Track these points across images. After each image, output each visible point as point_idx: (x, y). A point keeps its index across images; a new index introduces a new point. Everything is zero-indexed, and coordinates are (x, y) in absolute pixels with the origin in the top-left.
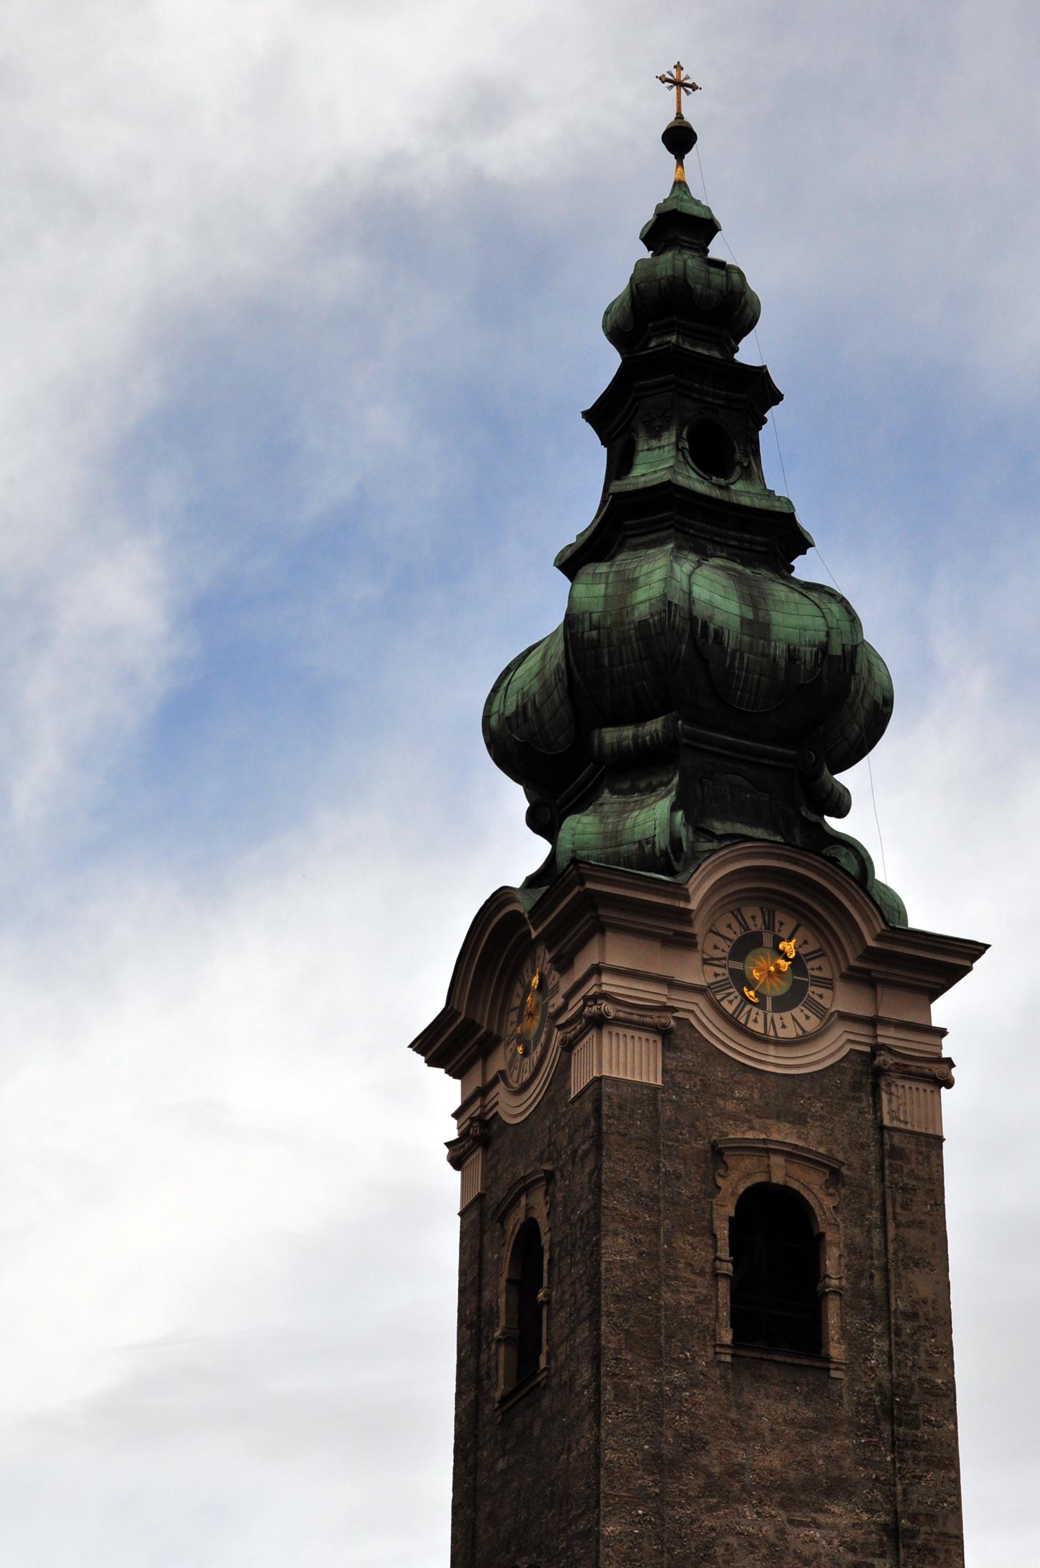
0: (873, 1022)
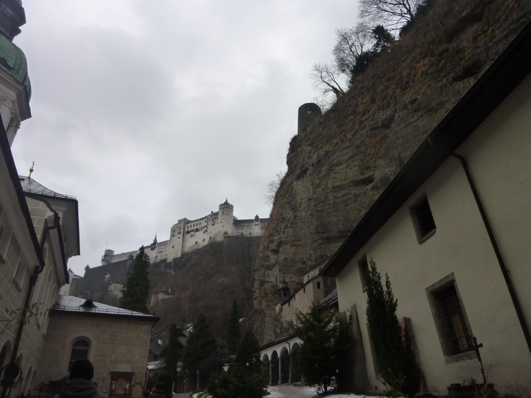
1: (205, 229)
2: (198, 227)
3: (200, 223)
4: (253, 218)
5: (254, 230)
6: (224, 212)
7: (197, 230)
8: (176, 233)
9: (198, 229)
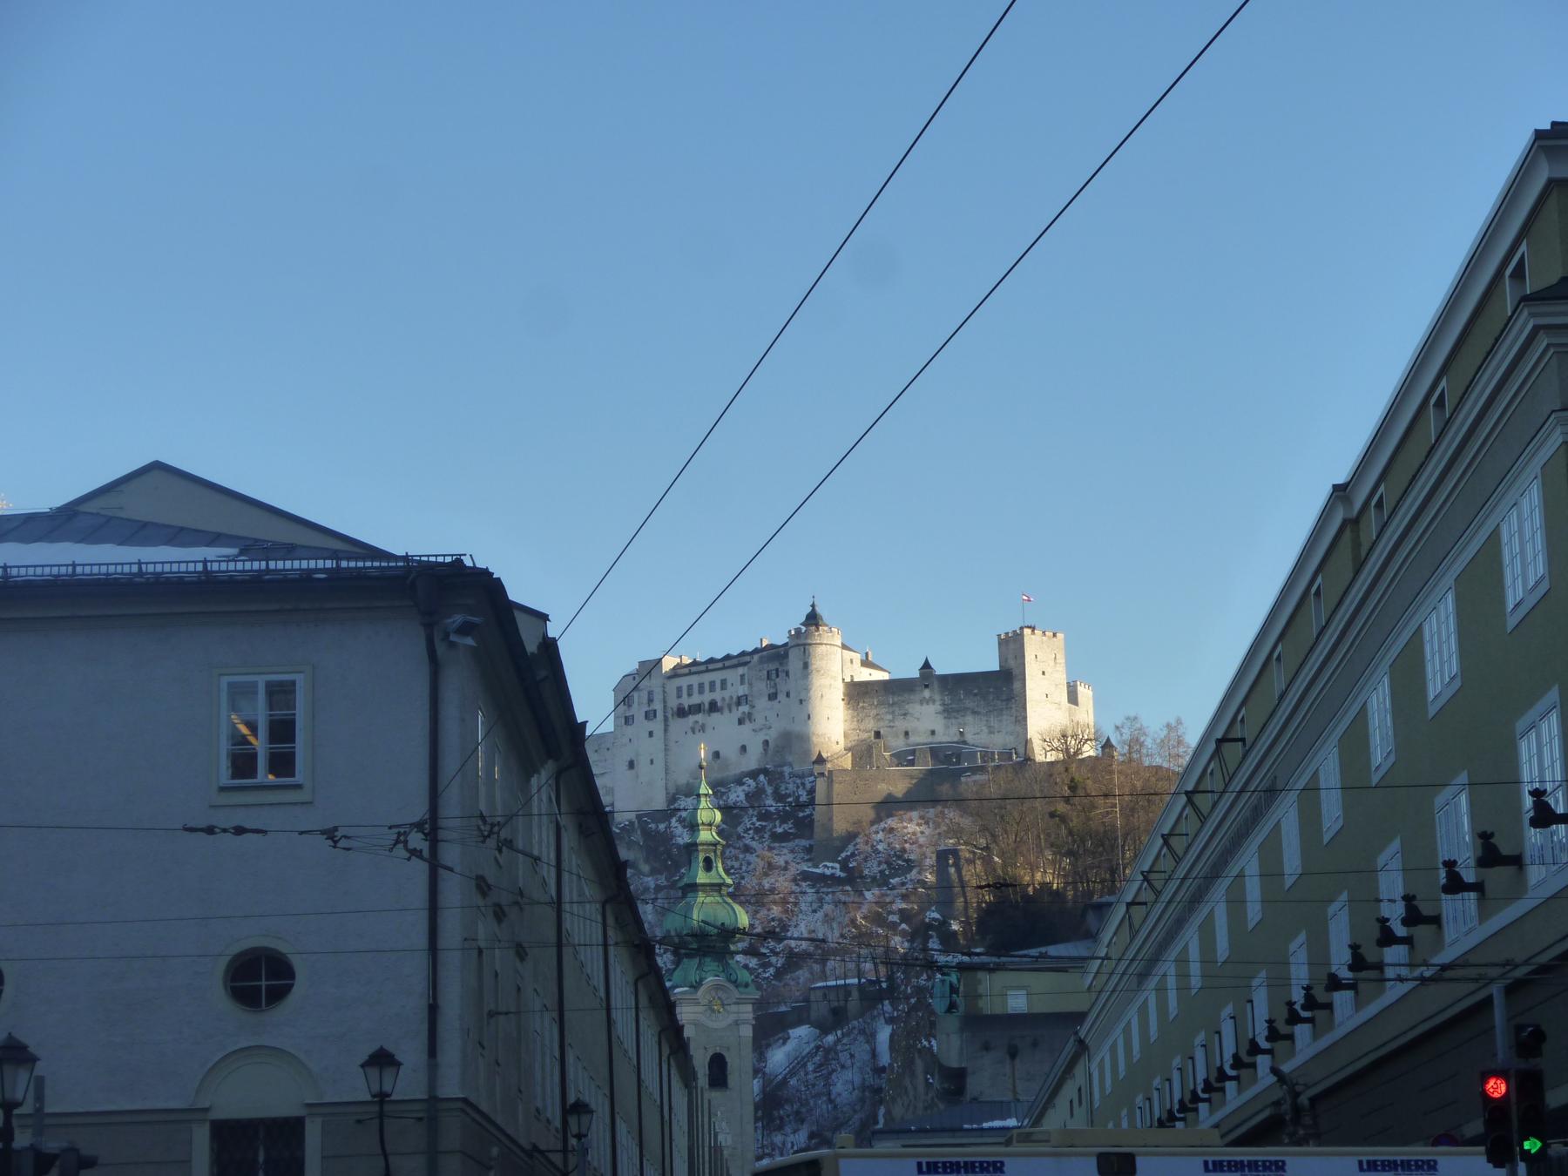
0: (738, 1013)
1: (745, 708)
2: (717, 695)
3: (724, 682)
4: (915, 673)
7: (714, 707)
8: (638, 711)
9: (719, 704)
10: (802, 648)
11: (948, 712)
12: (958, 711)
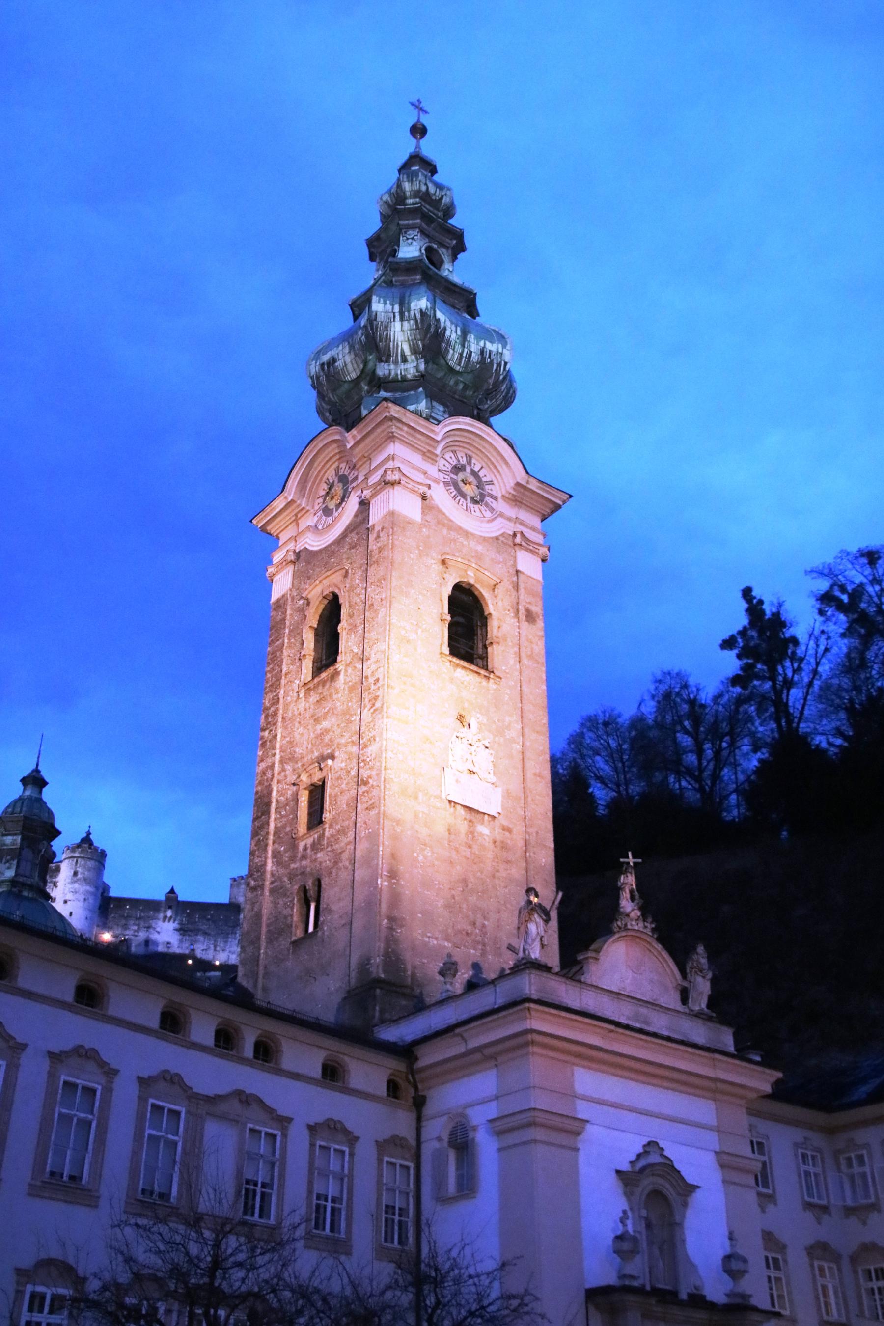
5: (159, 933)
6: (78, 869)
10: (75, 860)
11: (182, 930)
12: (191, 931)
